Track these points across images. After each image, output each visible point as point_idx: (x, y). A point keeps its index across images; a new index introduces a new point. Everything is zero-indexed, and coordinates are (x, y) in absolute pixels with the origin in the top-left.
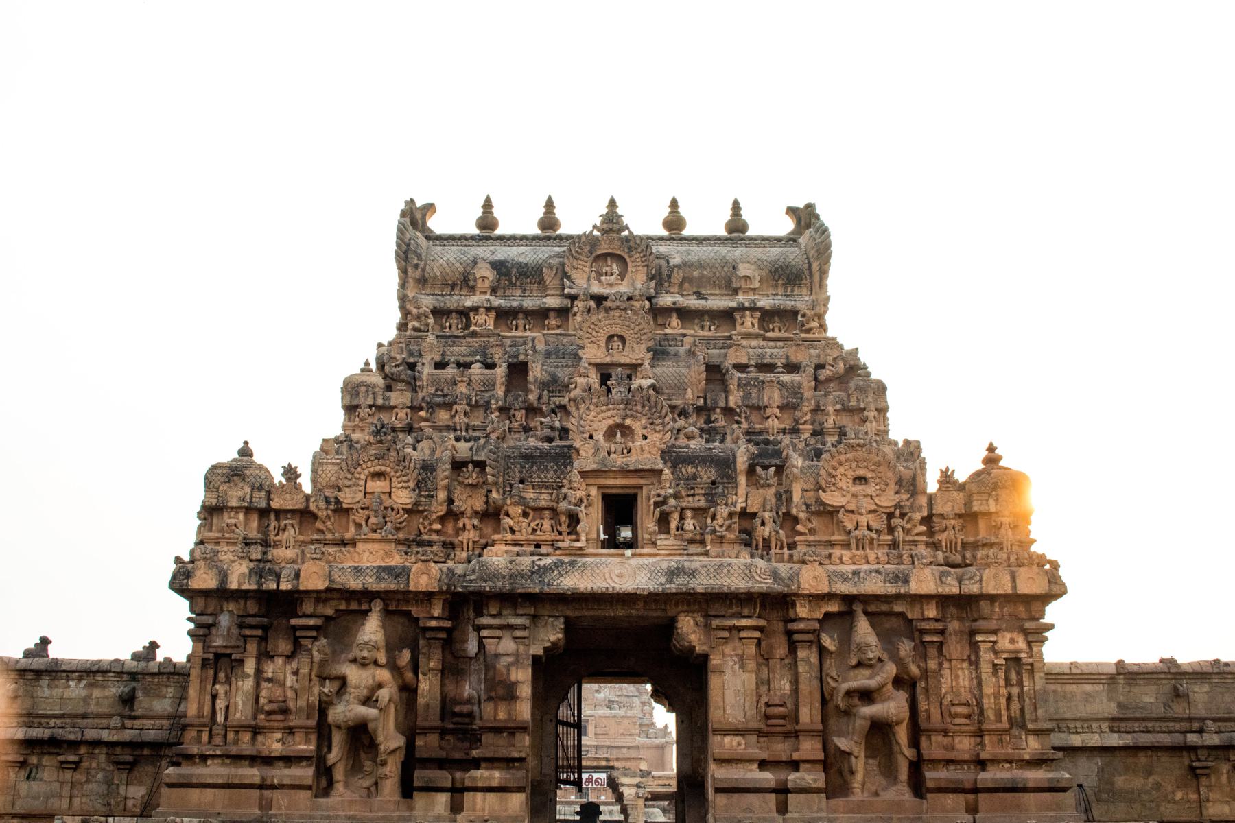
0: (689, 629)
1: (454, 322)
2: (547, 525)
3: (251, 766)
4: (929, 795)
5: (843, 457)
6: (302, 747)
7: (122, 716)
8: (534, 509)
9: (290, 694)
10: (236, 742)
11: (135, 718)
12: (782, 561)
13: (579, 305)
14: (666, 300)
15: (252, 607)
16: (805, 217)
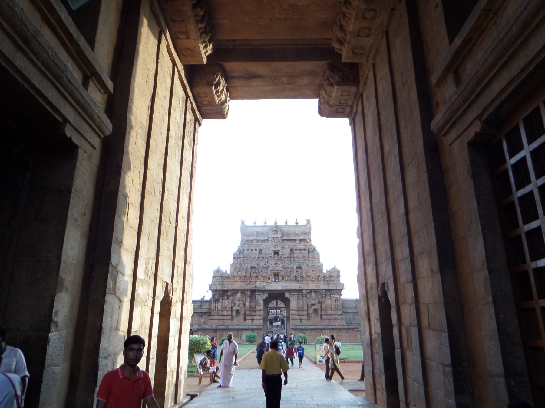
0: (287, 295)
1: (250, 242)
2: (265, 278)
3: (222, 316)
4: (323, 320)
5: (311, 267)
6: (229, 313)
7: (200, 308)
8: (263, 276)
9: (227, 305)
10: (219, 313)
11: (202, 308)
12: (301, 284)
13: (270, 239)
14: (284, 238)
15: (221, 292)
16: (308, 221)
